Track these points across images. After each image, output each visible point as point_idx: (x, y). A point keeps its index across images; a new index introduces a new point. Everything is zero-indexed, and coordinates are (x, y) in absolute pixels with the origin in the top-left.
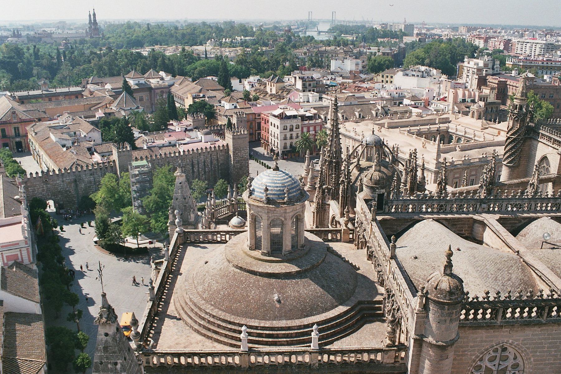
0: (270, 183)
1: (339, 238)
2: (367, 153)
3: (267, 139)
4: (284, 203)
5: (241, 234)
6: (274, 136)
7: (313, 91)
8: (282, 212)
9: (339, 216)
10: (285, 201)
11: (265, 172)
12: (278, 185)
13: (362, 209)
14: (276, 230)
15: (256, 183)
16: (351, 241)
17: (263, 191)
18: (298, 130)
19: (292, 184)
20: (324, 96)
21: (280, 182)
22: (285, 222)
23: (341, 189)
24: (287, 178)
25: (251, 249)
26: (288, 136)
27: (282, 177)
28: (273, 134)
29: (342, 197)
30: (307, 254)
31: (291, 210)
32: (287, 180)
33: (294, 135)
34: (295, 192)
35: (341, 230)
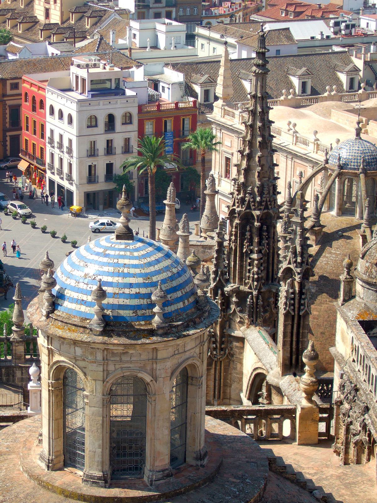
0: (109, 274)
1: (287, 432)
2: (341, 191)
3: (38, 155)
4: (152, 333)
5: (15, 426)
6: (61, 146)
7: (169, 16)
8: (144, 356)
9: (278, 369)
10: (155, 325)
11: (92, 244)
12: (132, 280)
13: (355, 350)
14: (123, 411)
15: (69, 276)
16: (326, 440)
17: (90, 298)
18: (129, 127)
19: (172, 278)
20: (199, 30)
21: (137, 271)
22: (153, 387)
23: (283, 294)
24: (158, 261)
25: (52, 466)
26: (101, 147)
27: (144, 256)
28: (57, 139)
29: (286, 315)
30: (211, 479)
31: (171, 350)
32: (157, 267)
33: (118, 144)
34: (180, 299)
35: (293, 411)
